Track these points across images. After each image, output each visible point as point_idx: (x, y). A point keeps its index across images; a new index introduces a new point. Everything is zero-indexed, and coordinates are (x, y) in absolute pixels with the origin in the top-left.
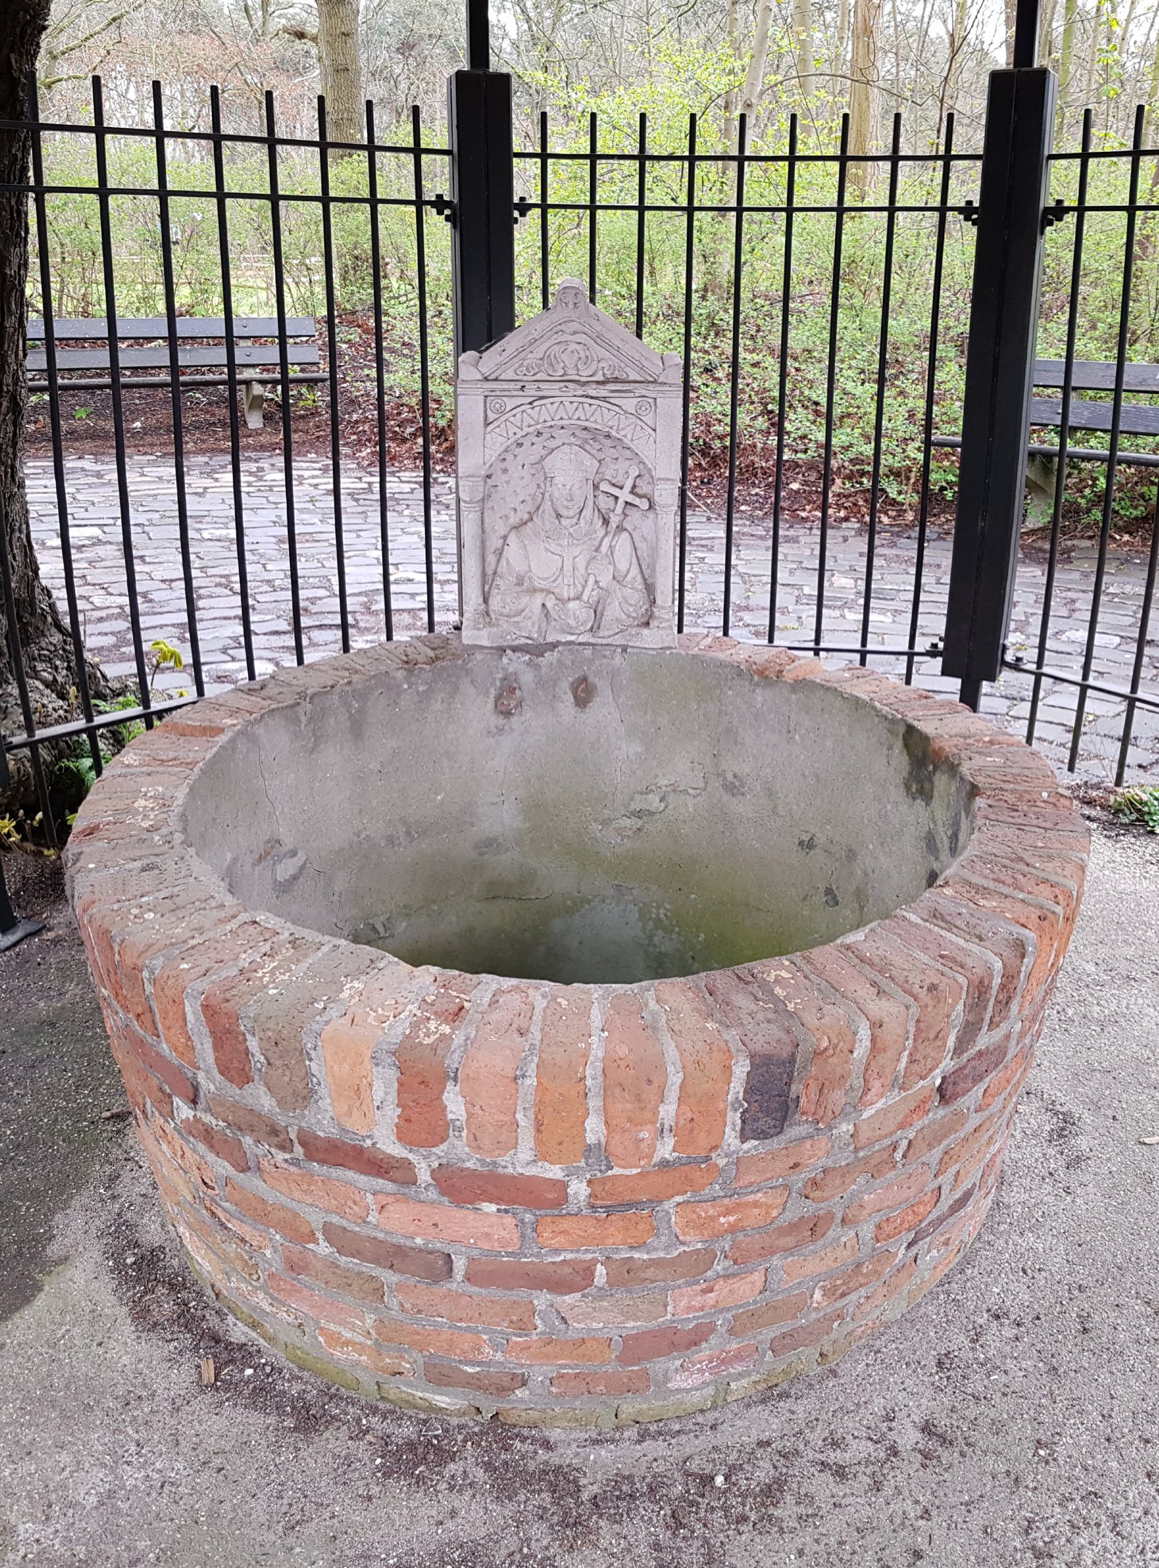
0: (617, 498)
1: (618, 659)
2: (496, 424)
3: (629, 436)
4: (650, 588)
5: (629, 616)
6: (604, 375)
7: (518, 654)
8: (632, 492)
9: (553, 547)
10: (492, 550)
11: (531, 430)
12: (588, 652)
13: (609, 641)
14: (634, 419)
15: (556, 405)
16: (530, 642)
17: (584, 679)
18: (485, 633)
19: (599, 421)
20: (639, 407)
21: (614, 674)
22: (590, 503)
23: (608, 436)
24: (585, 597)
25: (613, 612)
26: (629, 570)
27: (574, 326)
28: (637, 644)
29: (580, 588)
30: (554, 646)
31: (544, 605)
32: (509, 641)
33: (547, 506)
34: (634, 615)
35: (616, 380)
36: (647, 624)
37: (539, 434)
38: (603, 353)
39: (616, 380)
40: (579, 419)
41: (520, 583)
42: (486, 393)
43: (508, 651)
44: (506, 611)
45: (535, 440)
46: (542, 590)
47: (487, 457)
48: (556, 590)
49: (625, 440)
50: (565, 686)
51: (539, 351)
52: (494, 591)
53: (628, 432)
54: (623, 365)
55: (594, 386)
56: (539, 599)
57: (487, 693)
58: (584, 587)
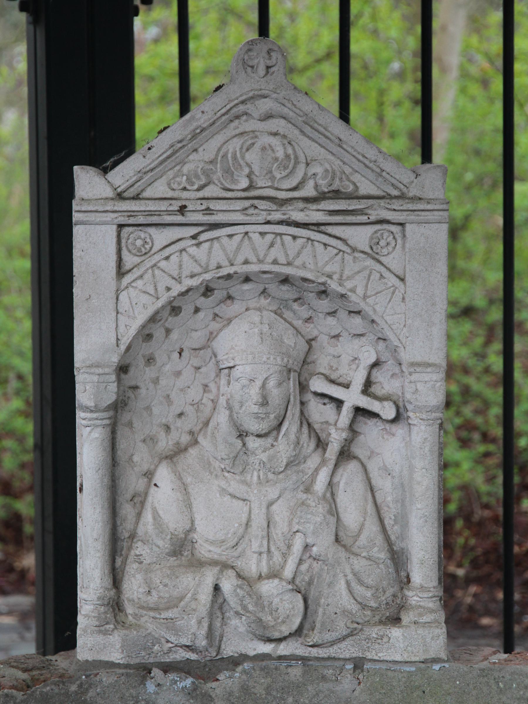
0: (339, 403)
1: (347, 683)
2: (136, 273)
3: (360, 291)
4: (398, 559)
5: (364, 607)
6: (316, 186)
7: (172, 676)
9: (235, 487)
10: (128, 496)
11: (194, 282)
13: (331, 651)
14: (369, 262)
15: (237, 239)
16: (193, 656)
18: (116, 639)
20: (375, 242)
22: (294, 411)
23: (323, 293)
25: (339, 598)
26: (362, 526)
27: (265, 106)
28: (382, 656)
29: (277, 557)
30: (235, 662)
31: (217, 588)
32: (159, 653)
33: (222, 418)
34: (373, 604)
35: (337, 194)
37: (208, 291)
38: (313, 149)
42: (123, 220)
43: (156, 672)
44: (153, 599)
45: (201, 301)
46: (214, 563)
47: (122, 329)
48: (239, 563)
49: (353, 297)
51: (210, 149)
52: (132, 567)
53: (359, 283)
54: (348, 170)
55: (301, 205)
56: (209, 577)
58: (285, 556)
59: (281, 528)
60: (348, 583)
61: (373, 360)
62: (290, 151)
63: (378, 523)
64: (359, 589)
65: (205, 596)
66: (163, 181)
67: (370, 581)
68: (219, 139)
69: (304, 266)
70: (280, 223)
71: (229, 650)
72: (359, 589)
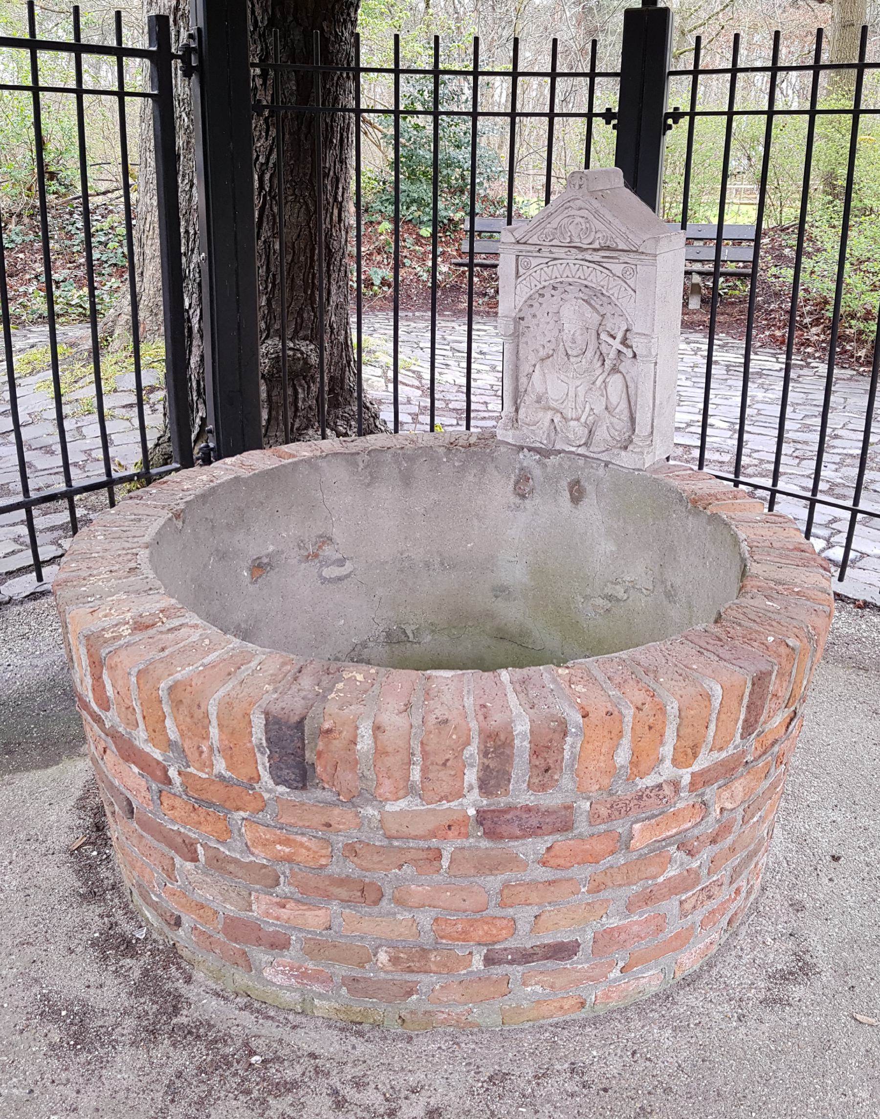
1: (601, 472)
3: (616, 295)
8: (621, 343)
10: (525, 374)
11: (546, 284)
12: (581, 462)
15: (564, 265)
17: (578, 482)
19: (594, 281)
20: (624, 272)
21: (598, 483)
24: (583, 420)
25: (601, 433)
28: (617, 463)
30: (559, 452)
31: (553, 420)
35: (608, 248)
36: (626, 448)
39: (608, 248)
40: (579, 278)
41: (538, 401)
46: (553, 409)
47: (517, 301)
48: (564, 411)
50: (564, 484)
53: (615, 291)
56: (549, 415)
57: (509, 477)
58: (583, 412)
59: (581, 399)
60: (608, 427)
61: (625, 328)
62: (588, 226)
63: (627, 403)
64: (612, 431)
65: (547, 422)
66: (536, 236)
67: (618, 428)
68: (560, 218)
69: (591, 281)
70: (582, 260)
71: (557, 447)
72: (612, 431)
